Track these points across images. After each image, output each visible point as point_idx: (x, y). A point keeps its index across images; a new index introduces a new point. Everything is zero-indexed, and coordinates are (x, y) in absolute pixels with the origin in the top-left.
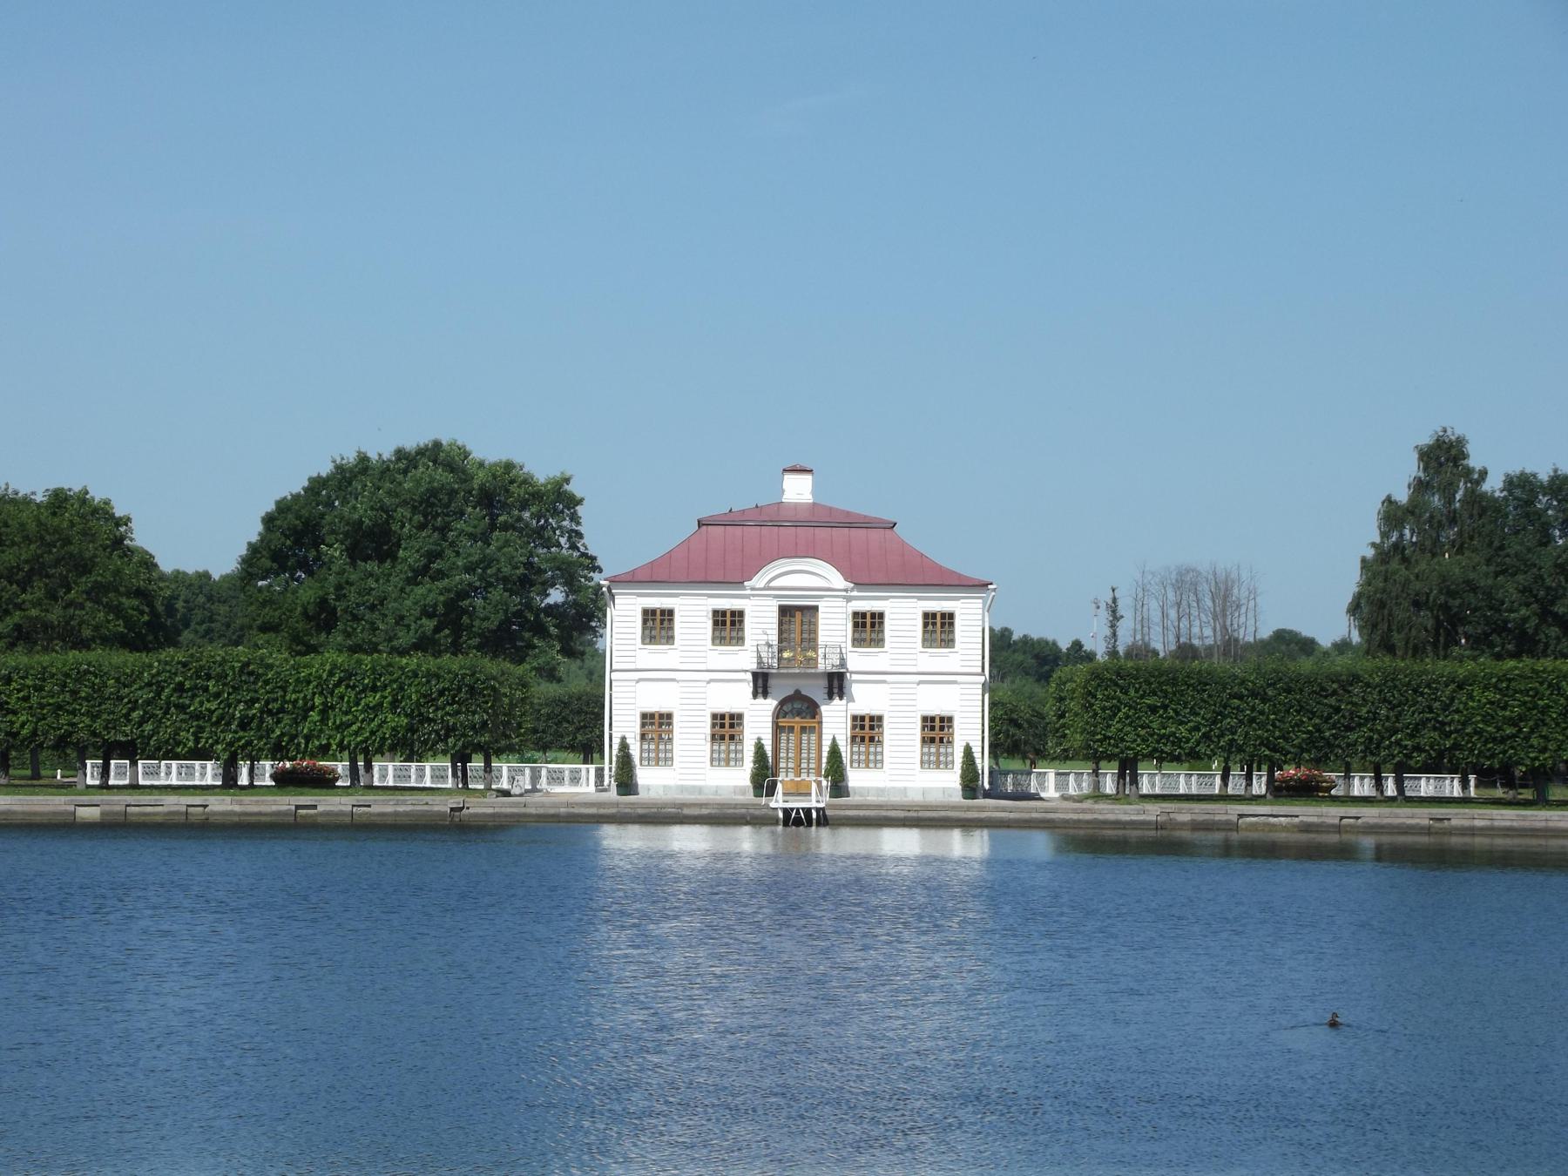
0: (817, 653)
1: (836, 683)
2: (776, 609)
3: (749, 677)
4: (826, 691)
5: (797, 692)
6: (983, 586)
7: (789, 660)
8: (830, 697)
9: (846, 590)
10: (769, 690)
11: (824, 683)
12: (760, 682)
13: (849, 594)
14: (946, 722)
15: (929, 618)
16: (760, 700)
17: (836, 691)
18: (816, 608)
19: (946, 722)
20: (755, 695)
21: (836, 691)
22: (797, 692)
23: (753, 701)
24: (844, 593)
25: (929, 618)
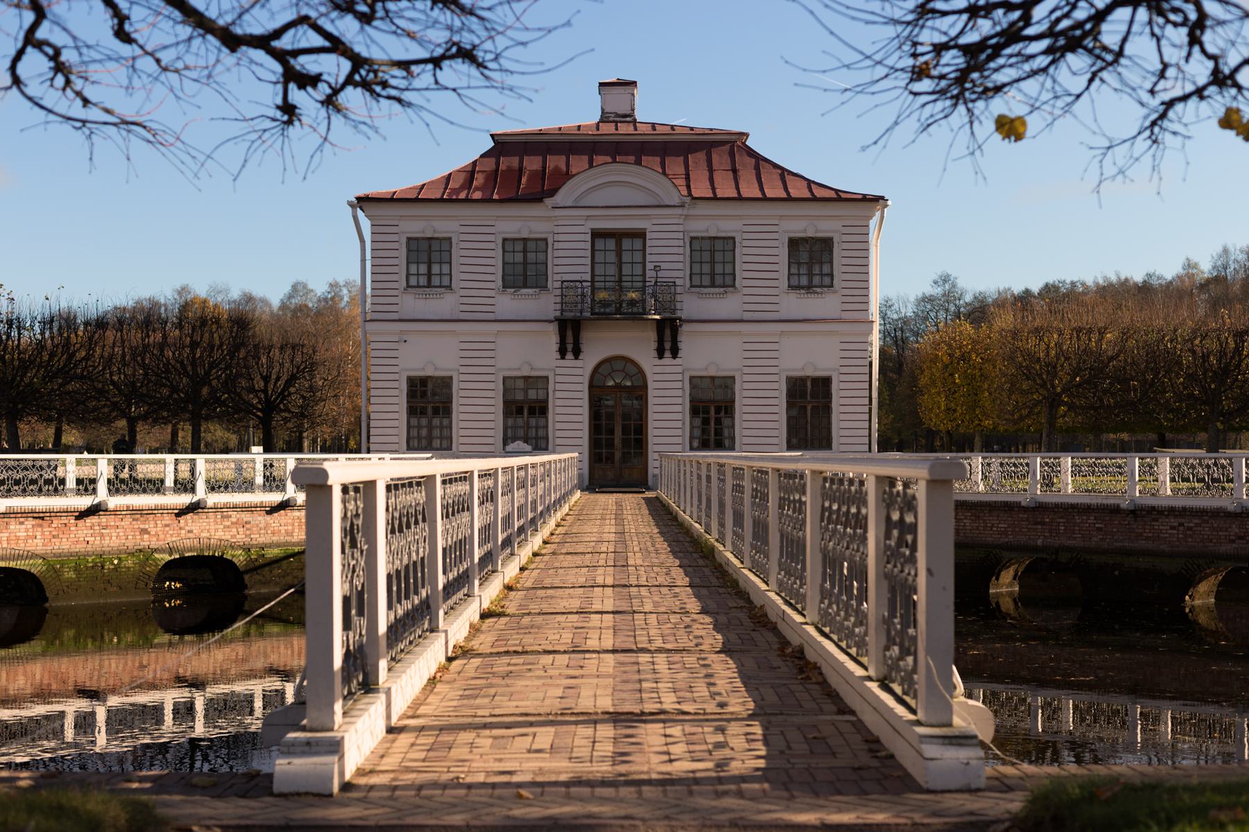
0: (643, 290)
1: (668, 332)
2: (588, 237)
3: (553, 329)
4: (654, 345)
7: (604, 304)
8: (661, 356)
10: (584, 347)
11: (652, 335)
12: (569, 334)
13: (685, 212)
14: (823, 385)
15: (794, 244)
16: (569, 361)
17: (668, 345)
18: (641, 235)
19: (823, 385)
20: (563, 353)
21: (668, 345)
23: (563, 363)
24: (679, 211)
25: (794, 244)
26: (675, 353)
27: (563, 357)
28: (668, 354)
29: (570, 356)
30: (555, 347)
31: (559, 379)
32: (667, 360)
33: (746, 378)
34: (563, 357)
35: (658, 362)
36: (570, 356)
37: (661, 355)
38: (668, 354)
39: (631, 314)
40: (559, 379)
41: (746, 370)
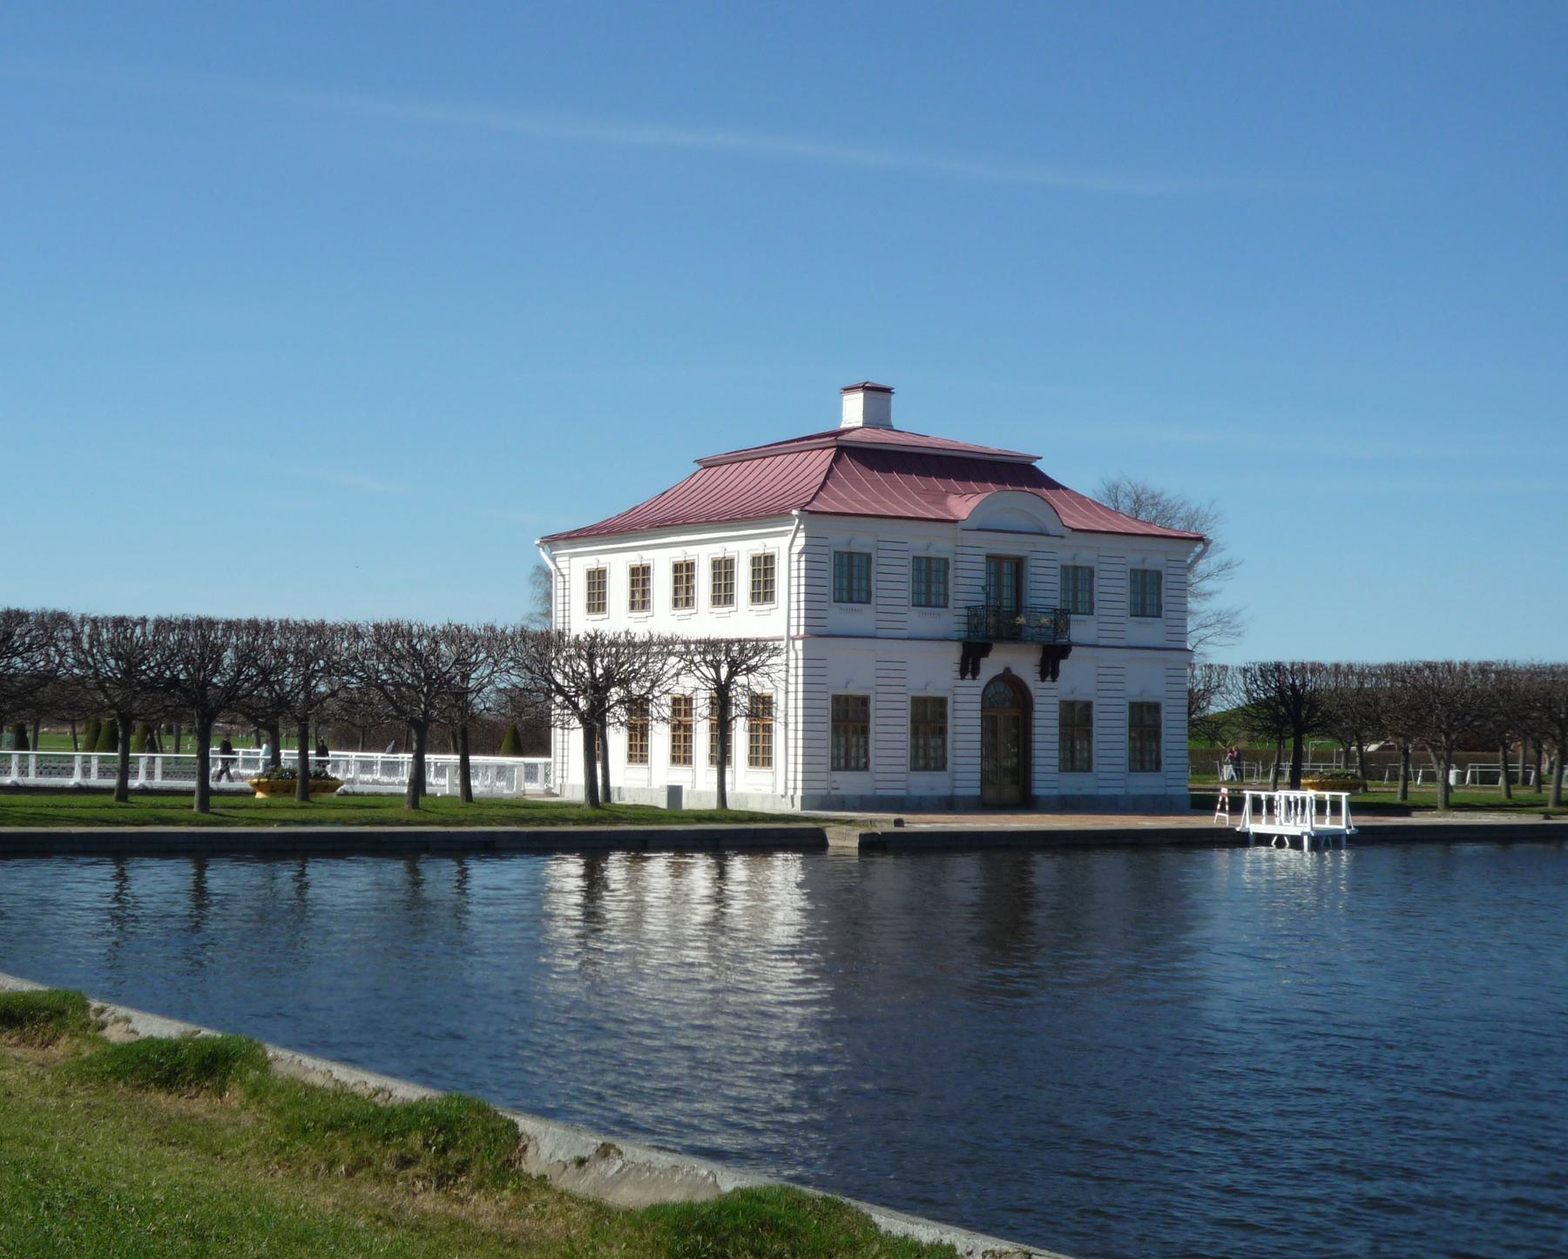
2: (983, 559)
5: (1007, 670)
6: (1200, 539)
8: (1043, 680)
9: (1062, 537)
14: (1155, 708)
16: (968, 682)
19: (1155, 708)
22: (1007, 670)
23: (961, 683)
26: (1055, 675)
27: (963, 678)
28: (1049, 678)
29: (969, 676)
30: (957, 667)
31: (880, 697)
32: (1048, 684)
33: (880, 697)
34: (963, 678)
35: (1041, 684)
36: (969, 676)
37: (1043, 680)
38: (1049, 678)
39: (1014, 636)
40: (959, 698)
41: (880, 689)
